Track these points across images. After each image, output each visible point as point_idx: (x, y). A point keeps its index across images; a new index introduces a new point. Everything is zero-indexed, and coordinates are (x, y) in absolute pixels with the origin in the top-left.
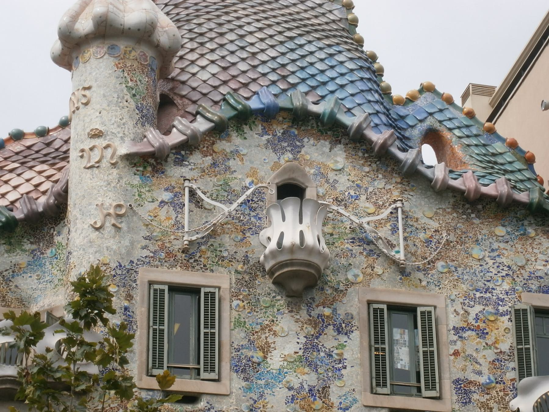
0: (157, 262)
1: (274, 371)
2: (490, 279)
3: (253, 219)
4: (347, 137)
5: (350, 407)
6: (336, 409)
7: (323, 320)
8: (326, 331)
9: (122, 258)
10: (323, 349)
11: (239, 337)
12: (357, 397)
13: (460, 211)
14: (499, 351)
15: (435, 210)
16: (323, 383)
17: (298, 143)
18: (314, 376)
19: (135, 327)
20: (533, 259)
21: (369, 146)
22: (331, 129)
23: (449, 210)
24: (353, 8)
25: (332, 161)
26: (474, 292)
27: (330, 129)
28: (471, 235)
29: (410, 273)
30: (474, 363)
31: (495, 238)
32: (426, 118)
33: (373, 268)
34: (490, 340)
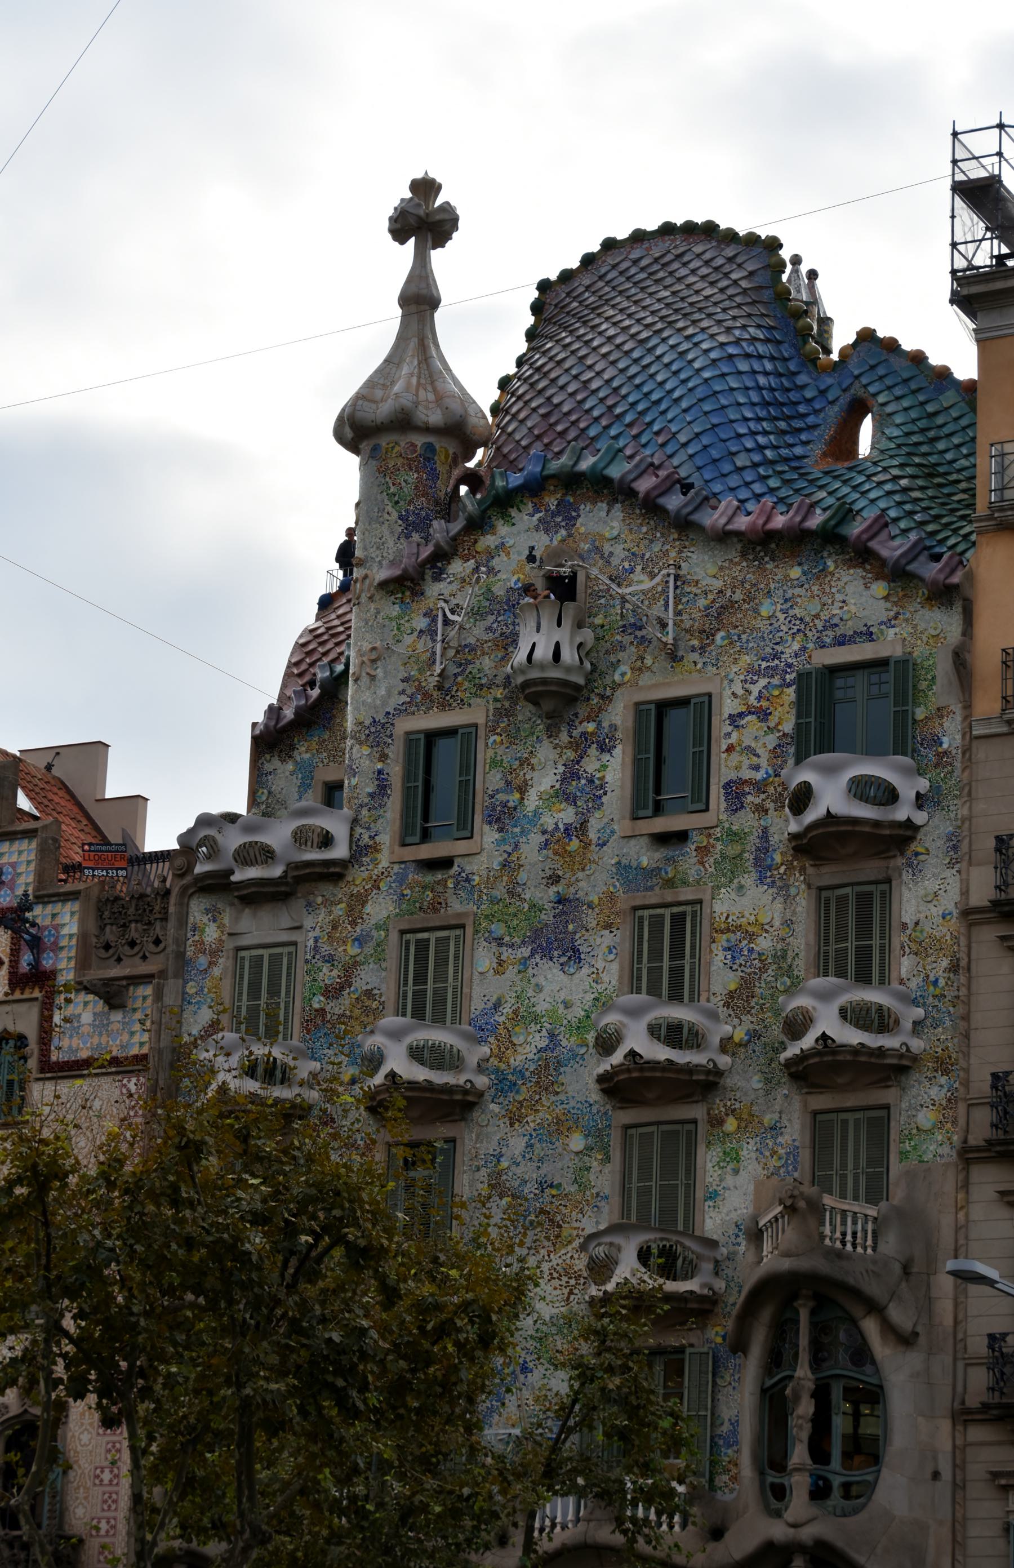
17: (574, 514)
22: (601, 487)
24: (781, 246)
27: (605, 487)
33: (643, 659)
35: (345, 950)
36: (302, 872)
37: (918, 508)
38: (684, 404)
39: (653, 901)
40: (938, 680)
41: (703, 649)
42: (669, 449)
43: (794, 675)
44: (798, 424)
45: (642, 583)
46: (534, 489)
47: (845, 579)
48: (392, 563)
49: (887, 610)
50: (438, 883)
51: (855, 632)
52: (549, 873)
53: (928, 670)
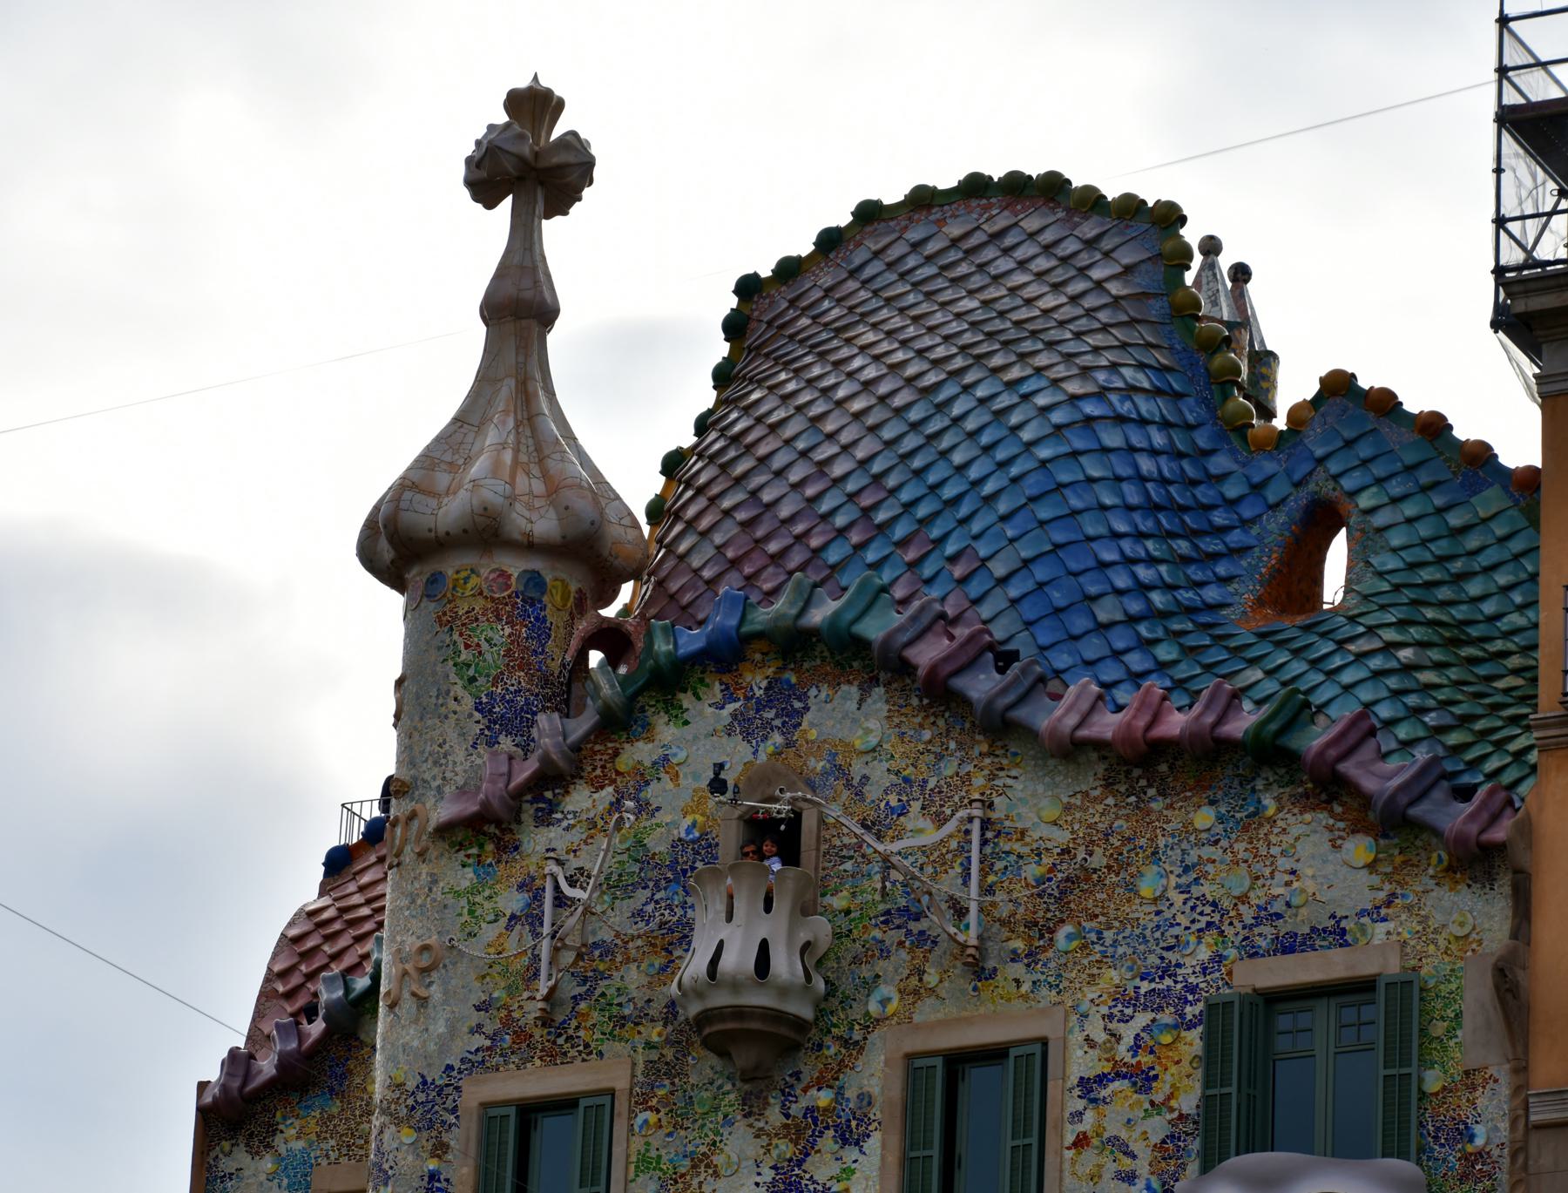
2: (1172, 941)
7: (815, 1120)
8: (820, 1143)
9: (429, 1065)
13: (1123, 789)
14: (1175, 1115)
15: (1065, 800)
17: (798, 705)
20: (1267, 872)
22: (849, 656)
23: (1097, 793)
24: (1183, 220)
26: (1137, 982)
28: (1143, 842)
29: (995, 969)
30: (1121, 1156)
31: (1192, 838)
32: (1310, 473)
33: (921, 973)
34: (1160, 1092)
37: (1431, 703)
38: (1003, 507)
40: (1467, 1020)
41: (1032, 956)
42: (974, 589)
43: (1201, 1006)
44: (1211, 545)
45: (920, 832)
46: (724, 657)
47: (1295, 831)
48: (462, 791)
49: (1372, 888)
51: (1313, 929)
53: (1449, 1000)
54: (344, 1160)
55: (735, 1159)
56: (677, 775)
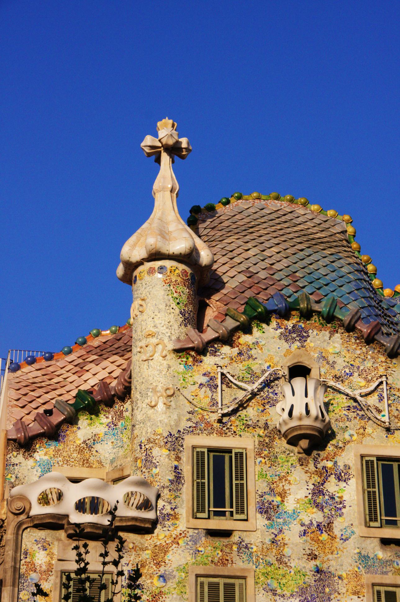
0: (198, 431)
1: (290, 512)
3: (271, 395)
4: (342, 328)
5: (350, 538)
6: (339, 540)
7: (327, 471)
8: (329, 479)
9: (172, 429)
10: (328, 494)
11: (263, 487)
12: (355, 530)
16: (327, 520)
17: (305, 334)
18: (320, 514)
19: (183, 481)
21: (359, 334)
25: (332, 347)
33: (365, 429)
35: (152, 583)
36: (124, 524)
39: (388, 582)
50: (226, 546)
52: (308, 552)
54: (65, 466)
55: (298, 479)
56: (262, 348)
